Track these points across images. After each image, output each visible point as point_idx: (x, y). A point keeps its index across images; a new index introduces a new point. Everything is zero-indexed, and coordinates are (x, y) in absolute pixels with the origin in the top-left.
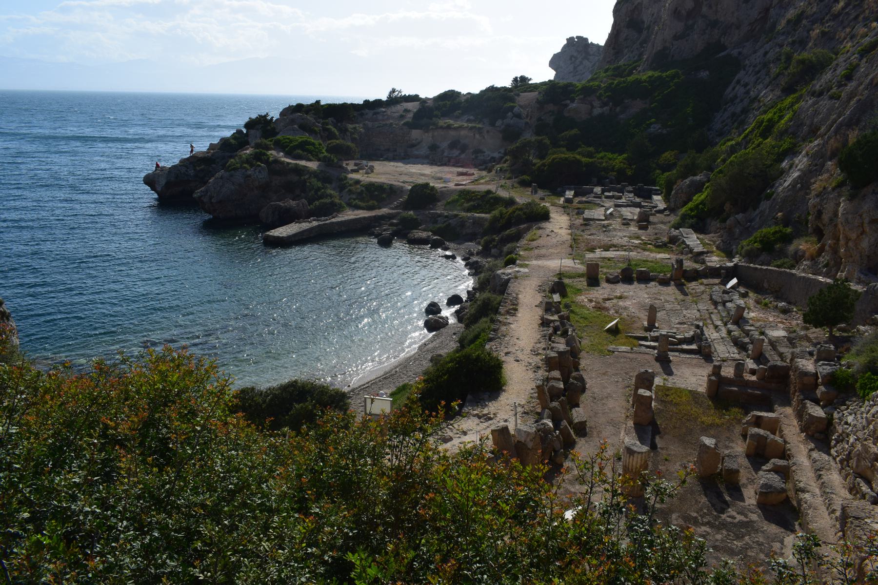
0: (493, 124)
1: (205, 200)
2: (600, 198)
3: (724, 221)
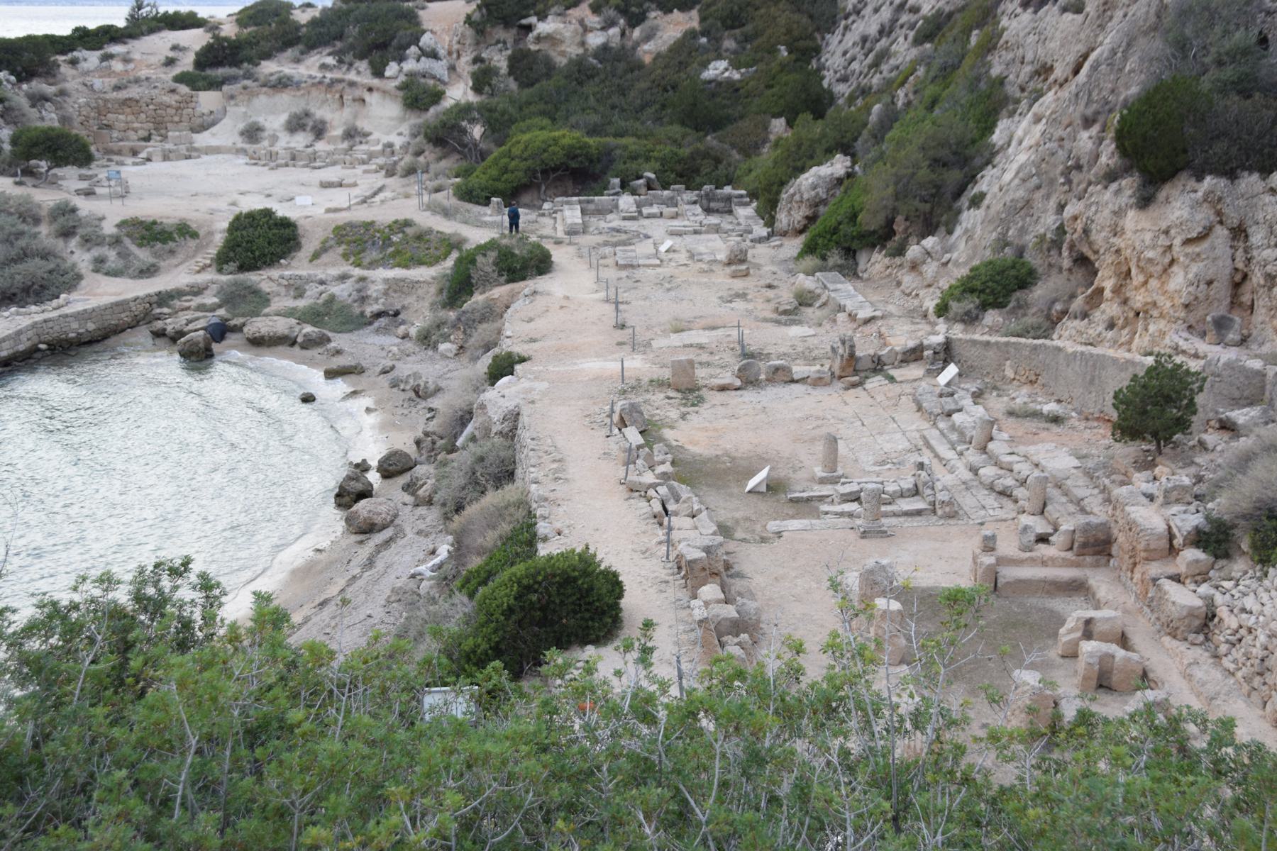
0: (378, 72)
3: (900, 251)
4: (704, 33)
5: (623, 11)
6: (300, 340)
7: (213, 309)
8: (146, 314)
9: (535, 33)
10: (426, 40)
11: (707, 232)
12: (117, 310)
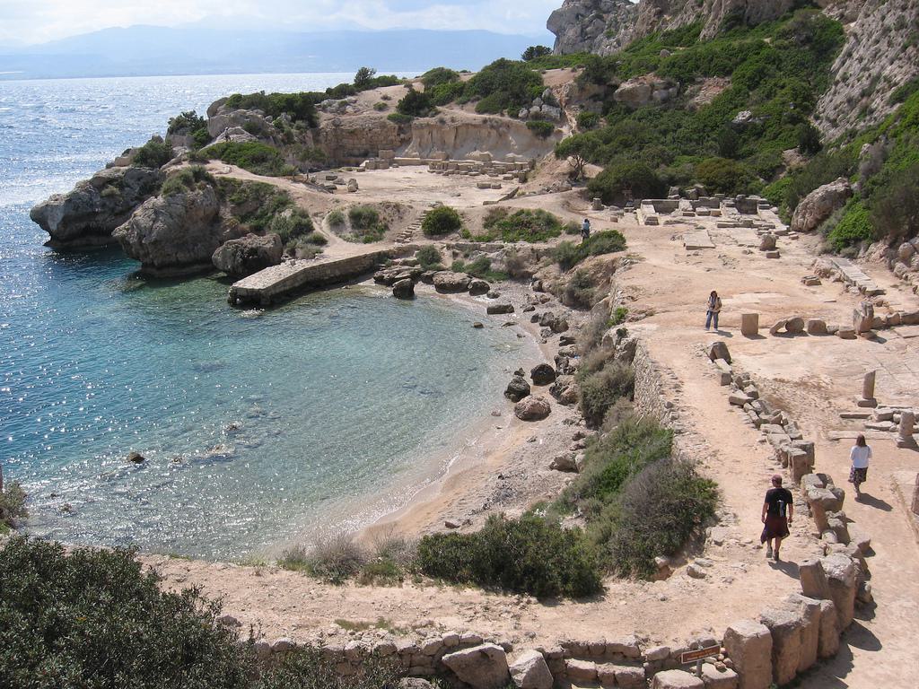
2: (693, 215)
6: (470, 287)
7: (414, 263)
8: (371, 267)
9: (619, 90)
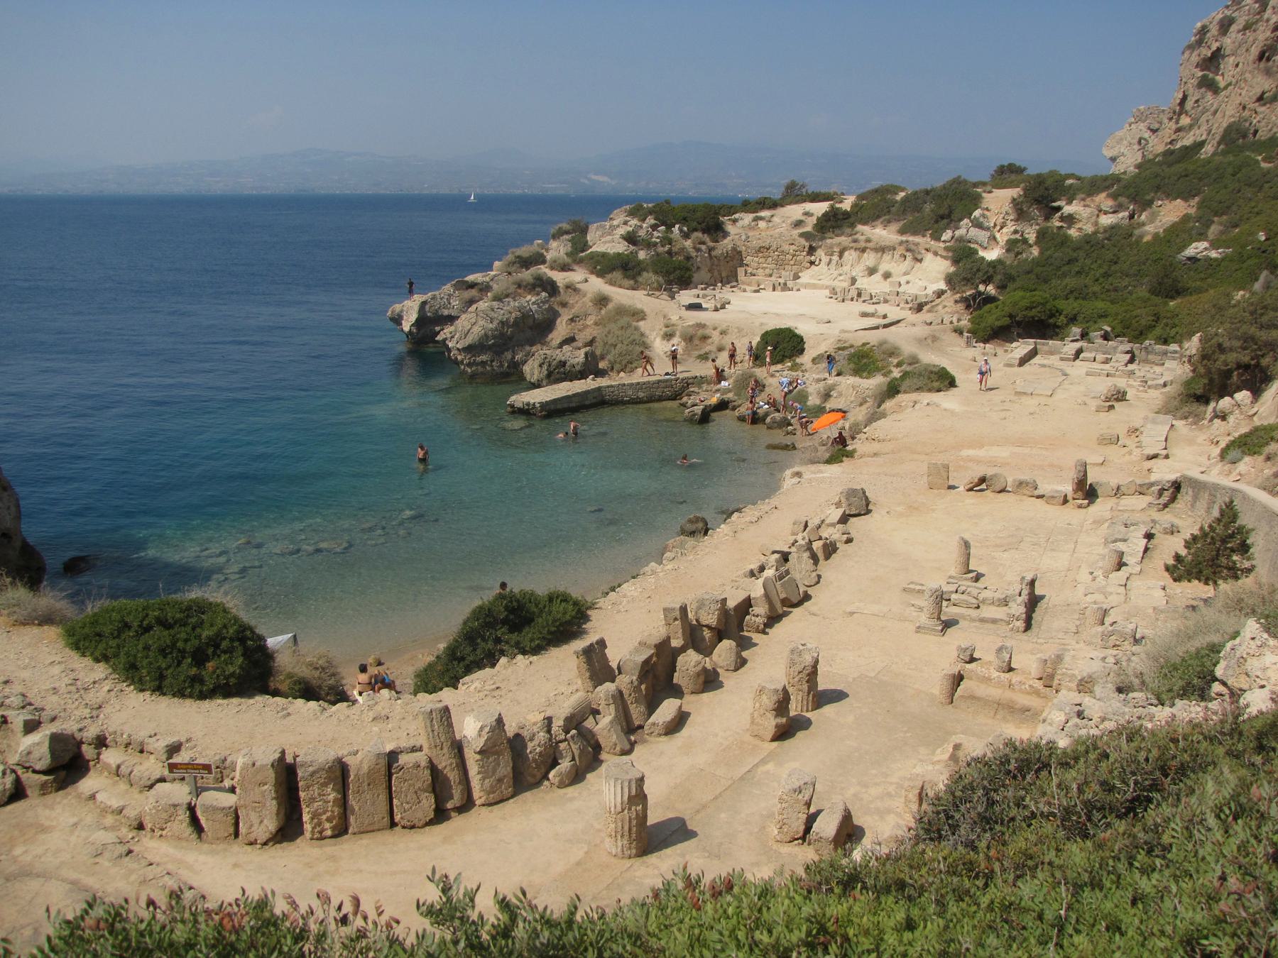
1: (450, 345)
4: (1199, 219)
5: (1133, 199)
10: (977, 213)
11: (1120, 377)
12: (663, 385)
